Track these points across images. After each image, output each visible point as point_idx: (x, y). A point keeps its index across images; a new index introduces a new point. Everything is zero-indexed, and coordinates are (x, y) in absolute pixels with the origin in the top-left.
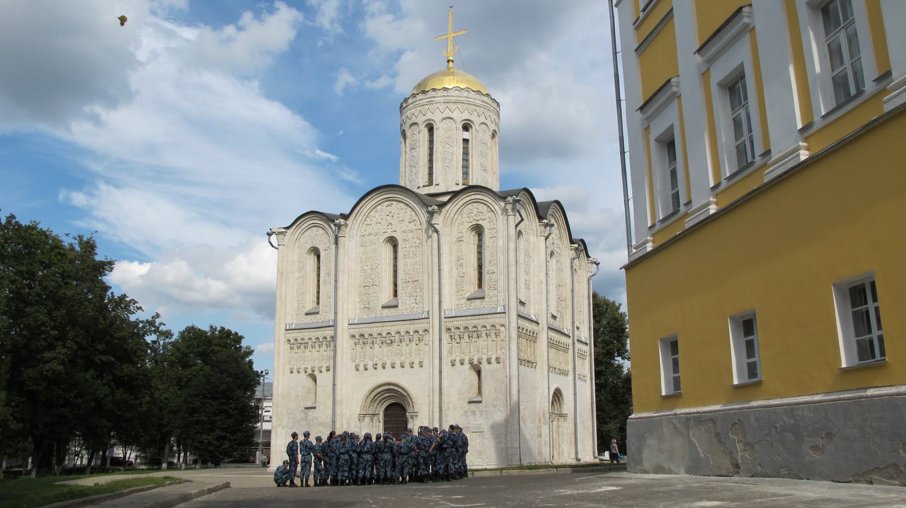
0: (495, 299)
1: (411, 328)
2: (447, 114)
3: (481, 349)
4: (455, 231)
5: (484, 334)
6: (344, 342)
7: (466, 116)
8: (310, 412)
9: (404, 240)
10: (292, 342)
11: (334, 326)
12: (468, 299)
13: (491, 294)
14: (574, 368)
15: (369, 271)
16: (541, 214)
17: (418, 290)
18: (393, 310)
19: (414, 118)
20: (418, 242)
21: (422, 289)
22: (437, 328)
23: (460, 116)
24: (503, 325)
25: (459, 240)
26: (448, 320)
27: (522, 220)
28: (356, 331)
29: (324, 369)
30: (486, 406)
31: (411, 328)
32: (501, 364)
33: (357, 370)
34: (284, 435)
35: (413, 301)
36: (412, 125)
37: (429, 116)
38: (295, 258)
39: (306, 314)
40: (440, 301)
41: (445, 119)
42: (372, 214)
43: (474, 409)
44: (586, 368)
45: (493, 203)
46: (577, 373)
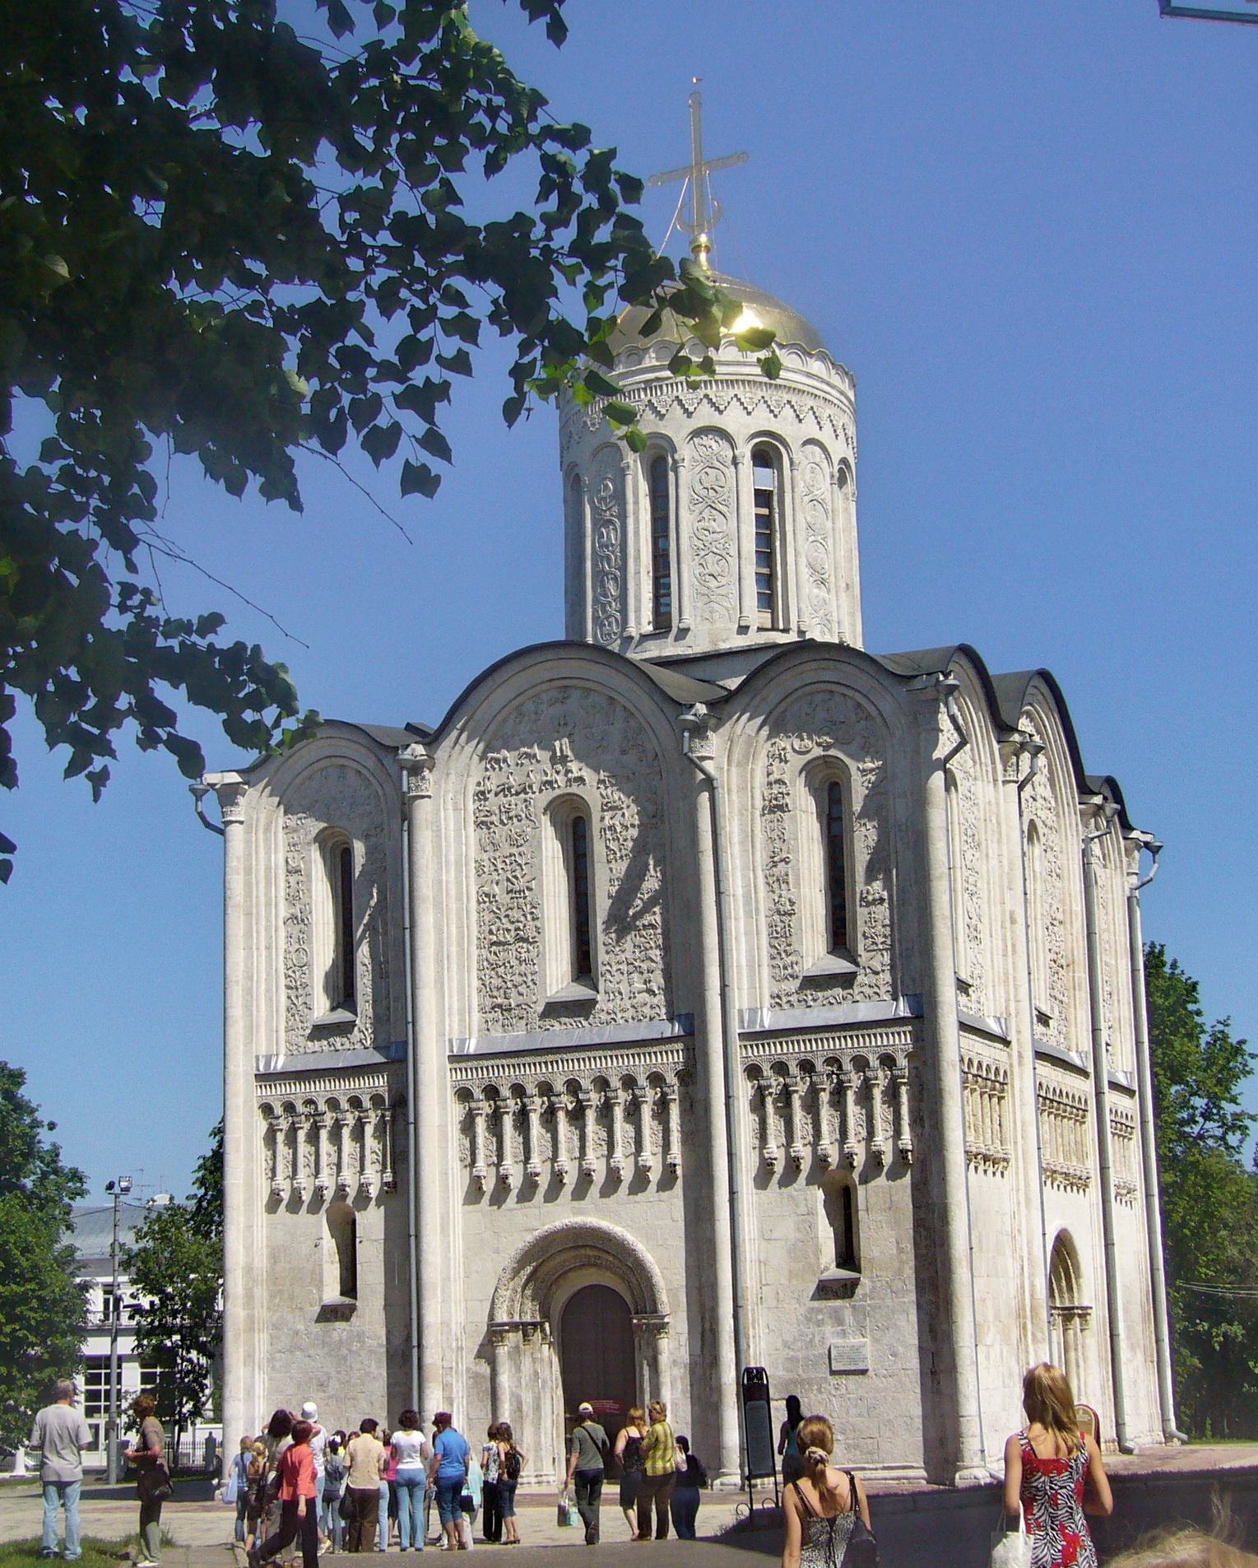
2: (705, 416)
4: (760, 778)
7: (763, 420)
14: (1104, 1169)
15: (503, 898)
16: (1005, 716)
23: (742, 424)
25: (776, 807)
27: (963, 743)
35: (639, 985)
40: (724, 986)
41: (698, 433)
44: (1131, 1163)
46: (1113, 1180)
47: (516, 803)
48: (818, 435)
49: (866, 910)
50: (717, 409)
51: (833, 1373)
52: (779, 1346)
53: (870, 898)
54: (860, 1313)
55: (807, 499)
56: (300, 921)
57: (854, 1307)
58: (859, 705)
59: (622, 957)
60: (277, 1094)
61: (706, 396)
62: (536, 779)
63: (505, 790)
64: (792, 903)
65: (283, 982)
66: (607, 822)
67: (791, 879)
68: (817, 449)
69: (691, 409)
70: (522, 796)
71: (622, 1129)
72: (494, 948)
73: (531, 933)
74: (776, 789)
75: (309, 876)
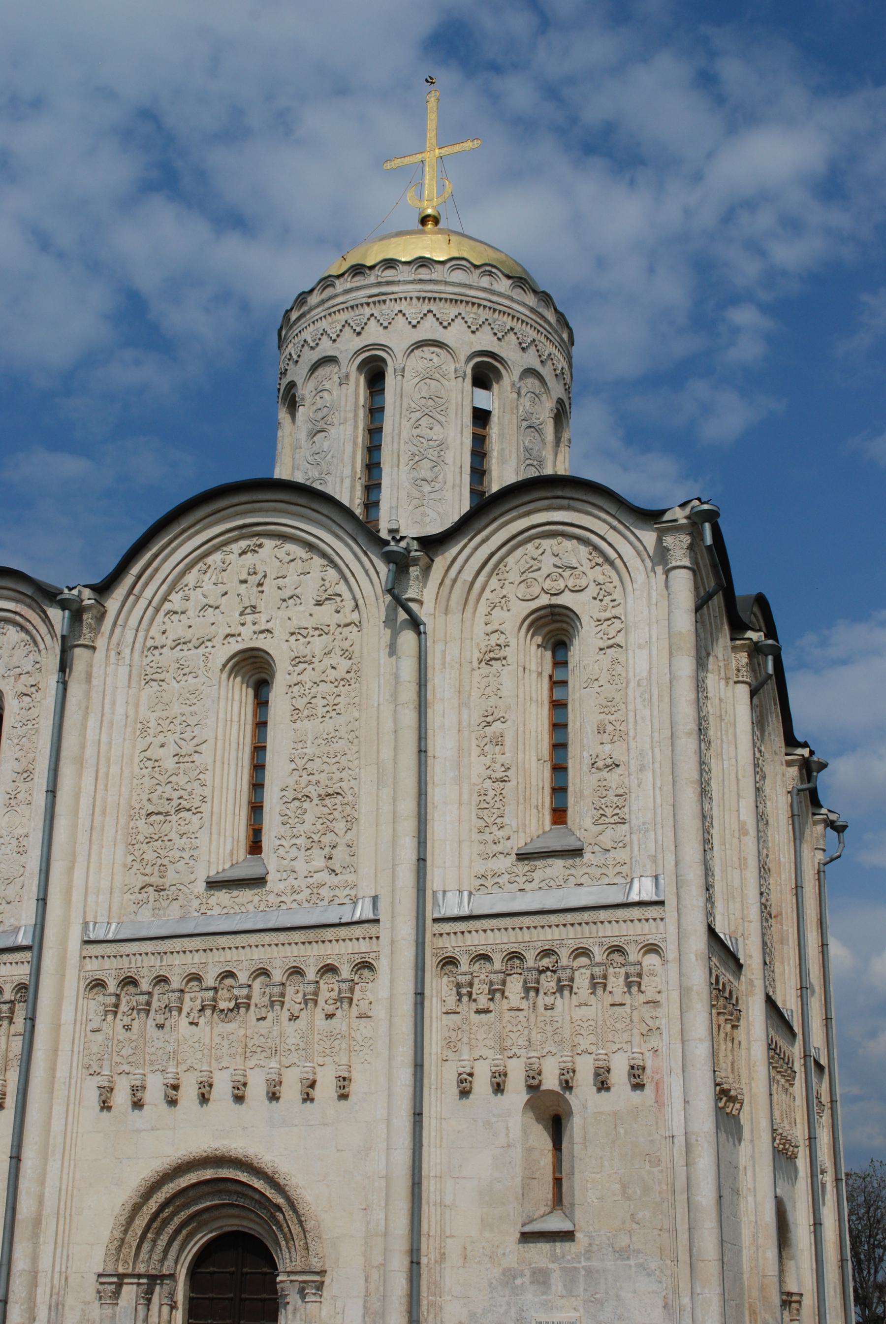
0: (621, 855)
1: (311, 956)
2: (429, 330)
3: (571, 1031)
5: (582, 981)
6: (64, 1003)
7: (485, 341)
9: (297, 660)
11: (35, 948)
12: (523, 857)
13: (606, 840)
15: (169, 764)
18: (245, 895)
19: (325, 343)
20: (345, 664)
21: (351, 821)
22: (407, 954)
23: (465, 340)
24: (652, 949)
26: (447, 927)
28: (110, 970)
30: (588, 1253)
31: (311, 956)
32: (649, 1090)
33: (105, 1106)
35: (319, 863)
36: (315, 367)
37: (374, 334)
40: (421, 860)
41: (420, 344)
42: (191, 578)
45: (612, 536)
48: (538, 367)
53: (600, 764)
55: (525, 424)
57: (562, 1269)
58: (596, 548)
59: (300, 829)
61: (430, 311)
66: (295, 678)
67: (508, 740)
68: (537, 383)
70: (202, 650)
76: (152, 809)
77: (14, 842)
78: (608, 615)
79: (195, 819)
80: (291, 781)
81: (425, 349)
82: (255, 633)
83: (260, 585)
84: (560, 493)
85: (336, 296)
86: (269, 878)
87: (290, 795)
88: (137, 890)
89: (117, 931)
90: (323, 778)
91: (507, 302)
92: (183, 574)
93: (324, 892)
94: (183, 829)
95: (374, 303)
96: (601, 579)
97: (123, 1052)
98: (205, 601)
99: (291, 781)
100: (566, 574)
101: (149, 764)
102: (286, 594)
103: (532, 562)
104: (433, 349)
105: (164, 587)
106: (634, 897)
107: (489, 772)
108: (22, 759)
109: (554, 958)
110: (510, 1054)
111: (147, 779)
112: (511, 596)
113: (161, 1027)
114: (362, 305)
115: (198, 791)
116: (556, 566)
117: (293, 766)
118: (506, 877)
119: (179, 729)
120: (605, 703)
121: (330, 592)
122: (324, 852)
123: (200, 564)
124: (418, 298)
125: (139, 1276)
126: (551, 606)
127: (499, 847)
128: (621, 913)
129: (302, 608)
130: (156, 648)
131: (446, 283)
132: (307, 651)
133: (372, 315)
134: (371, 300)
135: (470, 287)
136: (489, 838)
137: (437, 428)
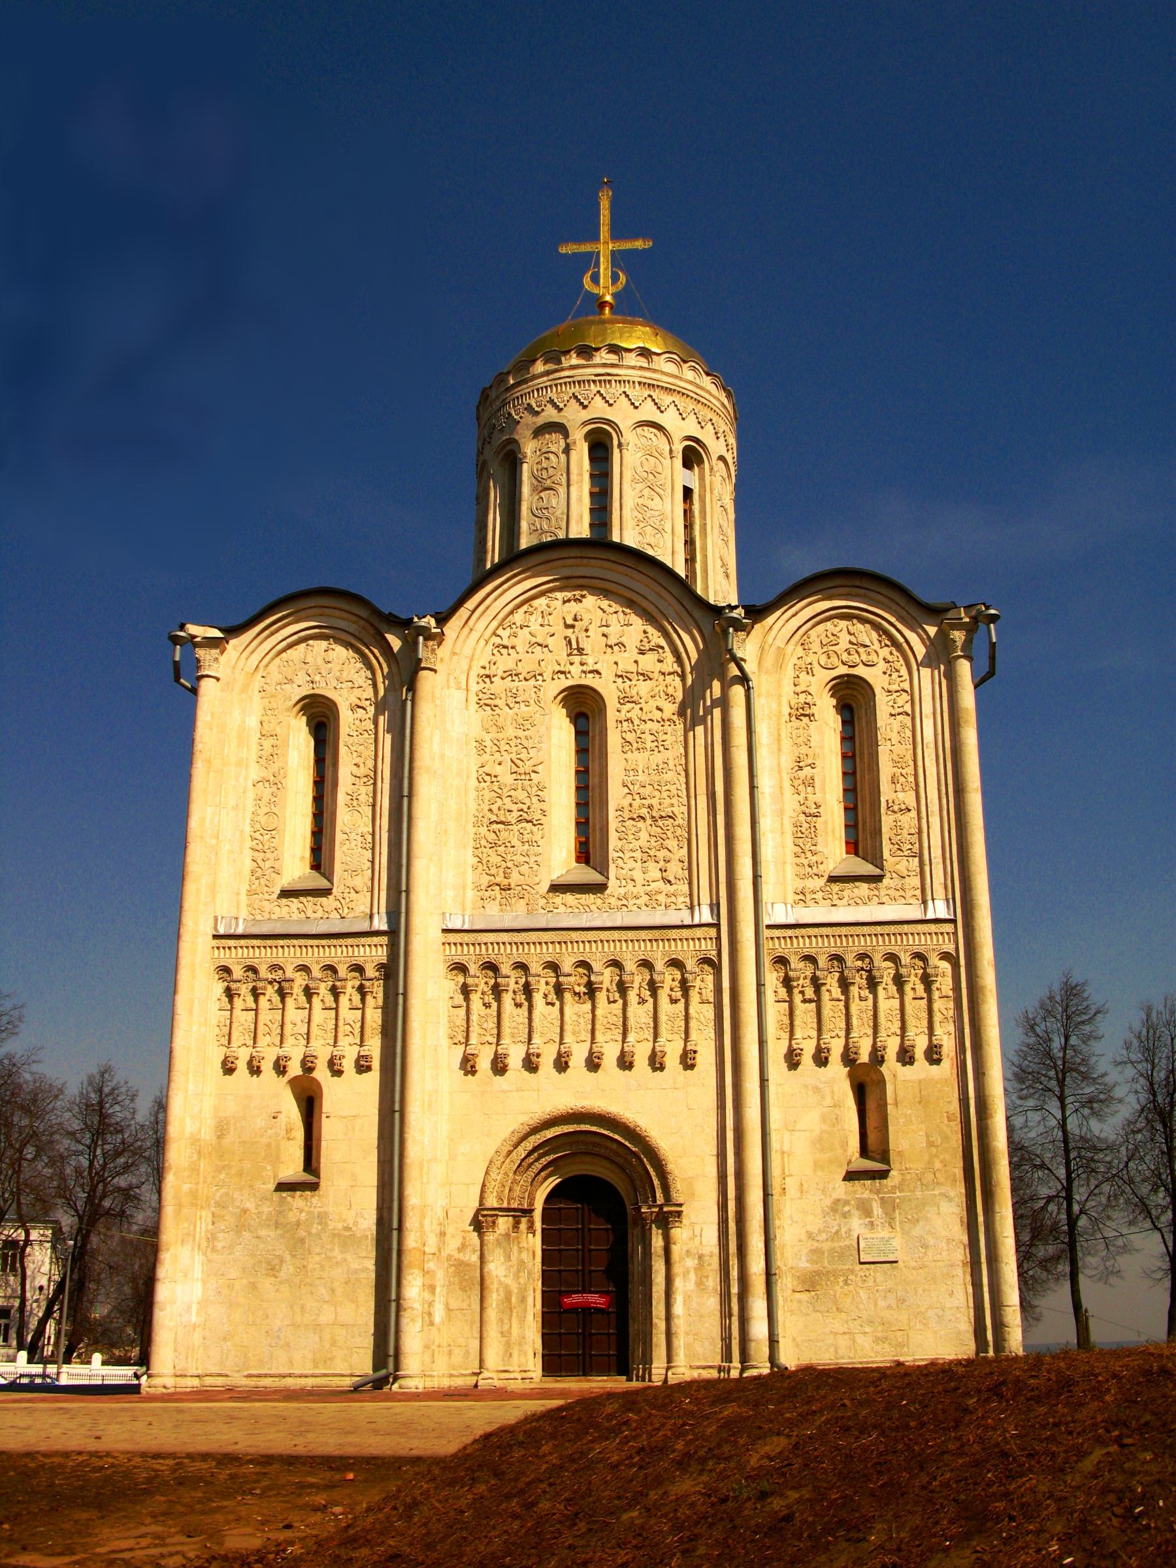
2: (648, 412)
4: (788, 689)
8: (297, 1201)
10: (238, 973)
12: (833, 879)
15: (508, 779)
17: (672, 844)
18: (589, 898)
25: (803, 713)
29: (348, 1065)
34: (198, 1273)
35: (658, 875)
37: (598, 409)
38: (253, 722)
39: (286, 894)
42: (519, 617)
43: (866, 1195)
47: (526, 688)
49: (893, 817)
50: (659, 408)
51: (861, 1263)
52: (804, 1237)
54: (890, 1207)
56: (275, 782)
57: (882, 1199)
60: (236, 957)
61: (650, 396)
62: (548, 669)
63: (512, 674)
64: (818, 807)
65: (249, 843)
66: (622, 716)
67: (817, 784)
69: (637, 404)
70: (532, 682)
71: (639, 1014)
72: (495, 826)
73: (537, 816)
74: (803, 696)
75: (286, 744)
76: (494, 818)
77: (360, 839)
78: (895, 687)
79: (535, 829)
80: (625, 803)
81: (646, 428)
82: (584, 672)
83: (587, 630)
84: (857, 583)
85: (562, 370)
86: (610, 884)
87: (627, 815)
88: (483, 887)
89: (471, 922)
90: (655, 802)
91: (707, 396)
92: (512, 612)
93: (662, 898)
94: (526, 837)
95: (600, 381)
96: (890, 658)
97: (485, 1026)
98: (534, 640)
99: (625, 803)
100: (861, 650)
101: (487, 778)
102: (612, 641)
103: (832, 638)
104: (652, 430)
105: (495, 624)
106: (930, 915)
107: (803, 808)
108: (362, 765)
109: (867, 960)
110: (834, 1034)
111: (486, 792)
112: (815, 664)
113: (518, 1005)
114: (588, 381)
115: (536, 805)
116: (851, 642)
117: (627, 791)
118: (821, 894)
119: (514, 749)
120: (896, 759)
121: (652, 643)
122: (659, 866)
123: (525, 608)
124: (640, 383)
125: (514, 1210)
126: (848, 675)
127: (815, 870)
128: (920, 928)
129: (626, 655)
130: (488, 676)
131: (663, 373)
132: (634, 692)
133: (599, 392)
134: (597, 378)
135: (681, 379)
136: (806, 862)
137: (657, 499)
